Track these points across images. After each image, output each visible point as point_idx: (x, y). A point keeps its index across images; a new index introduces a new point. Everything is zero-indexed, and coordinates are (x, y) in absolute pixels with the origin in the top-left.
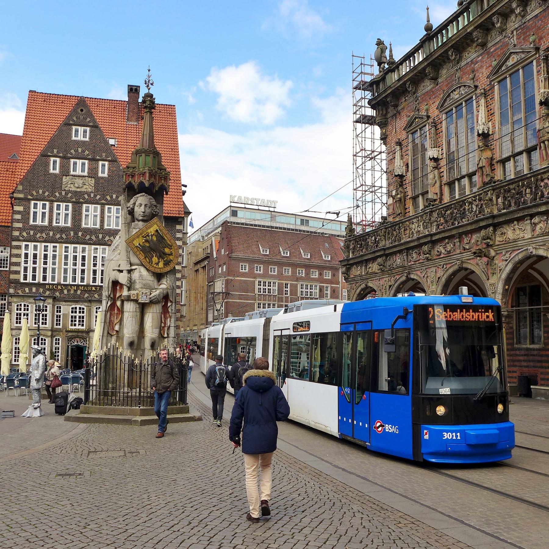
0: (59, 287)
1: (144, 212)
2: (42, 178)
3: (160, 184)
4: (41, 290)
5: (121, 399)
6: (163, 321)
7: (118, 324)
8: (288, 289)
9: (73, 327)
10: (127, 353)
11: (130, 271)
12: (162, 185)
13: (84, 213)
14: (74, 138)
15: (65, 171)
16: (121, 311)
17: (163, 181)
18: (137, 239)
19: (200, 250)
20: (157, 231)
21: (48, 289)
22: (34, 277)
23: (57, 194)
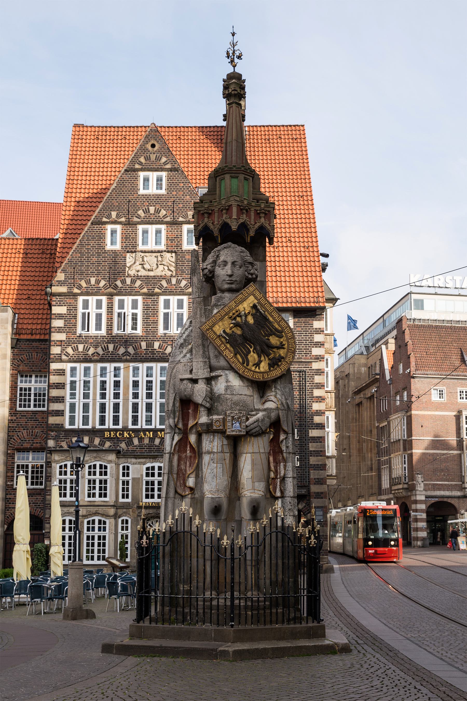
0: (126, 435)
1: (230, 276)
2: (95, 259)
3: (258, 224)
4: (97, 441)
5: (201, 611)
6: (273, 468)
7: (193, 475)
9: (150, 500)
11: (209, 380)
12: (262, 228)
13: (162, 310)
14: (142, 191)
15: (130, 246)
16: (197, 453)
17: (262, 220)
18: (220, 324)
19: (363, 369)
20: (254, 307)
21: (109, 439)
22: (86, 420)
23: (119, 283)
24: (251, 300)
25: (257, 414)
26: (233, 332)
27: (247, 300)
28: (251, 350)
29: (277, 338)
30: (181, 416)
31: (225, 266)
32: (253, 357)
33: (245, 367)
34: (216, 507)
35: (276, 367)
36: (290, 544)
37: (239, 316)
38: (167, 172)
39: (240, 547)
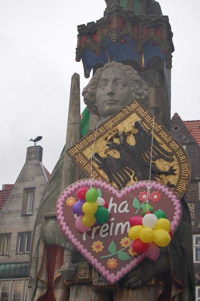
1: (111, 94)
18: (93, 146)
20: (137, 125)
24: (134, 118)
26: (108, 155)
28: (132, 177)
29: (166, 163)
30: (45, 265)
37: (117, 136)
38: (186, 146)
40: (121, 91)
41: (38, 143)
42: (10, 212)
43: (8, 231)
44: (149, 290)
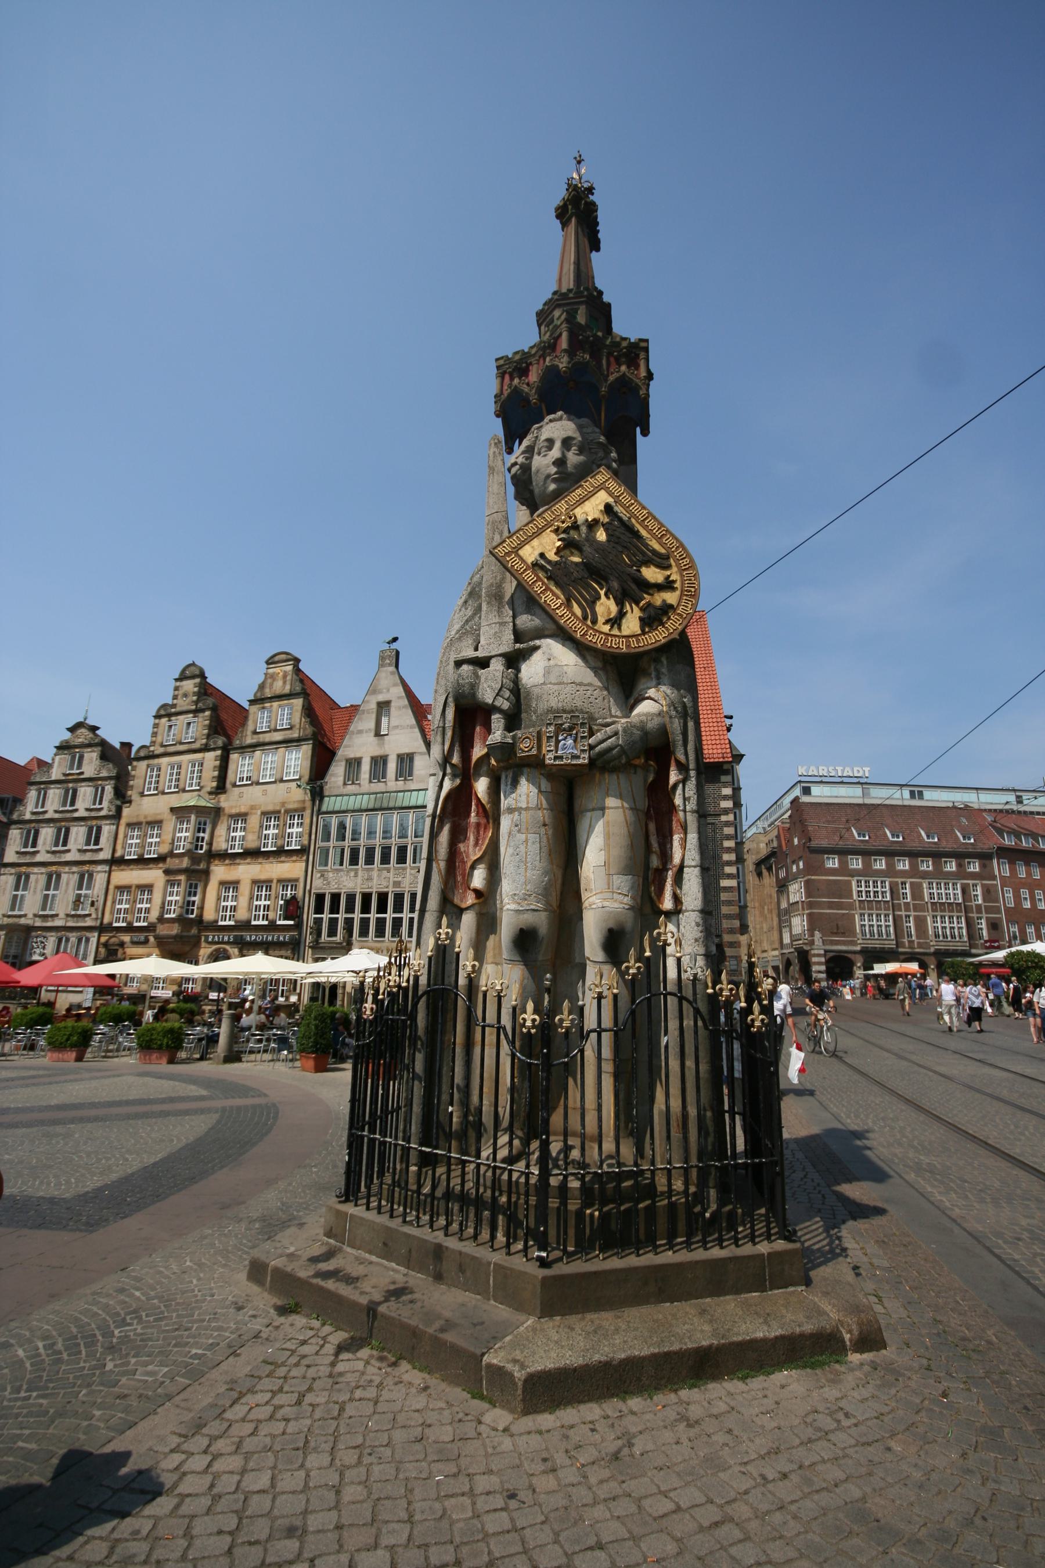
1: (560, 462)
6: (655, 846)
8: (908, 891)
10: (502, 977)
16: (492, 815)
18: (535, 542)
19: (762, 845)
20: (608, 509)
24: (602, 498)
25: (613, 723)
27: (592, 499)
28: (602, 593)
31: (550, 448)
32: (606, 606)
33: (588, 626)
34: (521, 930)
35: (656, 624)
36: (700, 1023)
39: (567, 1033)
40: (573, 458)
41: (394, 646)
42: (360, 732)
43: (358, 755)
44: (635, 773)
